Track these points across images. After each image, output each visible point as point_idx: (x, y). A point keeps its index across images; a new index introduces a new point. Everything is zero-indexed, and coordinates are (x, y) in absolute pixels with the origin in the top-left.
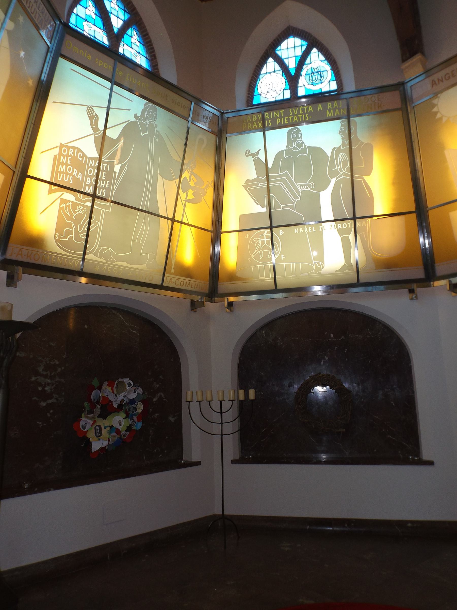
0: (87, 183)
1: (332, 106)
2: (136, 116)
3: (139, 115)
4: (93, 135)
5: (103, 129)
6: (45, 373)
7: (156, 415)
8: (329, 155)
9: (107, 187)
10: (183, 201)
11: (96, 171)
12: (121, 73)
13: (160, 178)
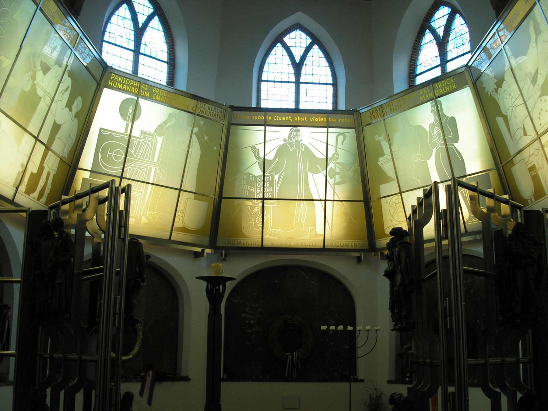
0: (258, 192)
1: (423, 92)
2: (285, 140)
3: (287, 138)
4: (257, 162)
5: (263, 156)
6: (250, 312)
7: (332, 343)
8: (428, 130)
9: (271, 191)
10: (332, 185)
11: (262, 183)
12: (270, 118)
13: (310, 174)
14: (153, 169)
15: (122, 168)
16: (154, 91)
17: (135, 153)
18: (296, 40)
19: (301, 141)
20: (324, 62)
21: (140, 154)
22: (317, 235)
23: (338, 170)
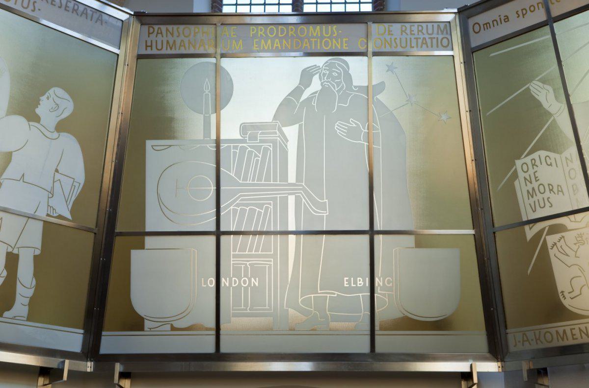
14: (291, 200)
15: (215, 214)
16: (252, 33)
17: (238, 174)
21: (250, 175)
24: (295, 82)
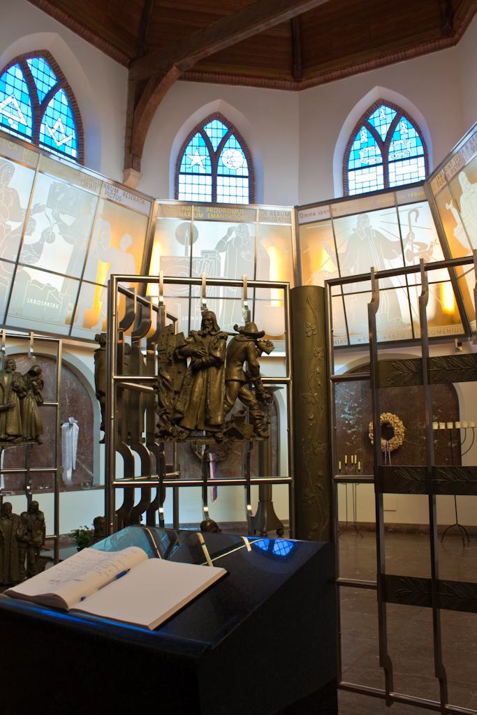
18: (381, 118)
19: (371, 227)
20: (413, 132)
22: (404, 325)
23: (416, 251)
24: (225, 233)
